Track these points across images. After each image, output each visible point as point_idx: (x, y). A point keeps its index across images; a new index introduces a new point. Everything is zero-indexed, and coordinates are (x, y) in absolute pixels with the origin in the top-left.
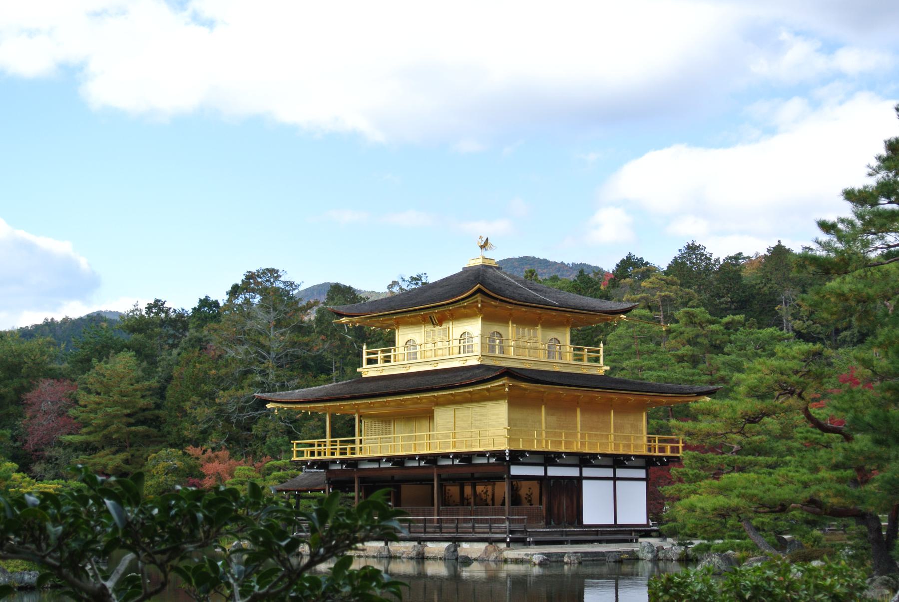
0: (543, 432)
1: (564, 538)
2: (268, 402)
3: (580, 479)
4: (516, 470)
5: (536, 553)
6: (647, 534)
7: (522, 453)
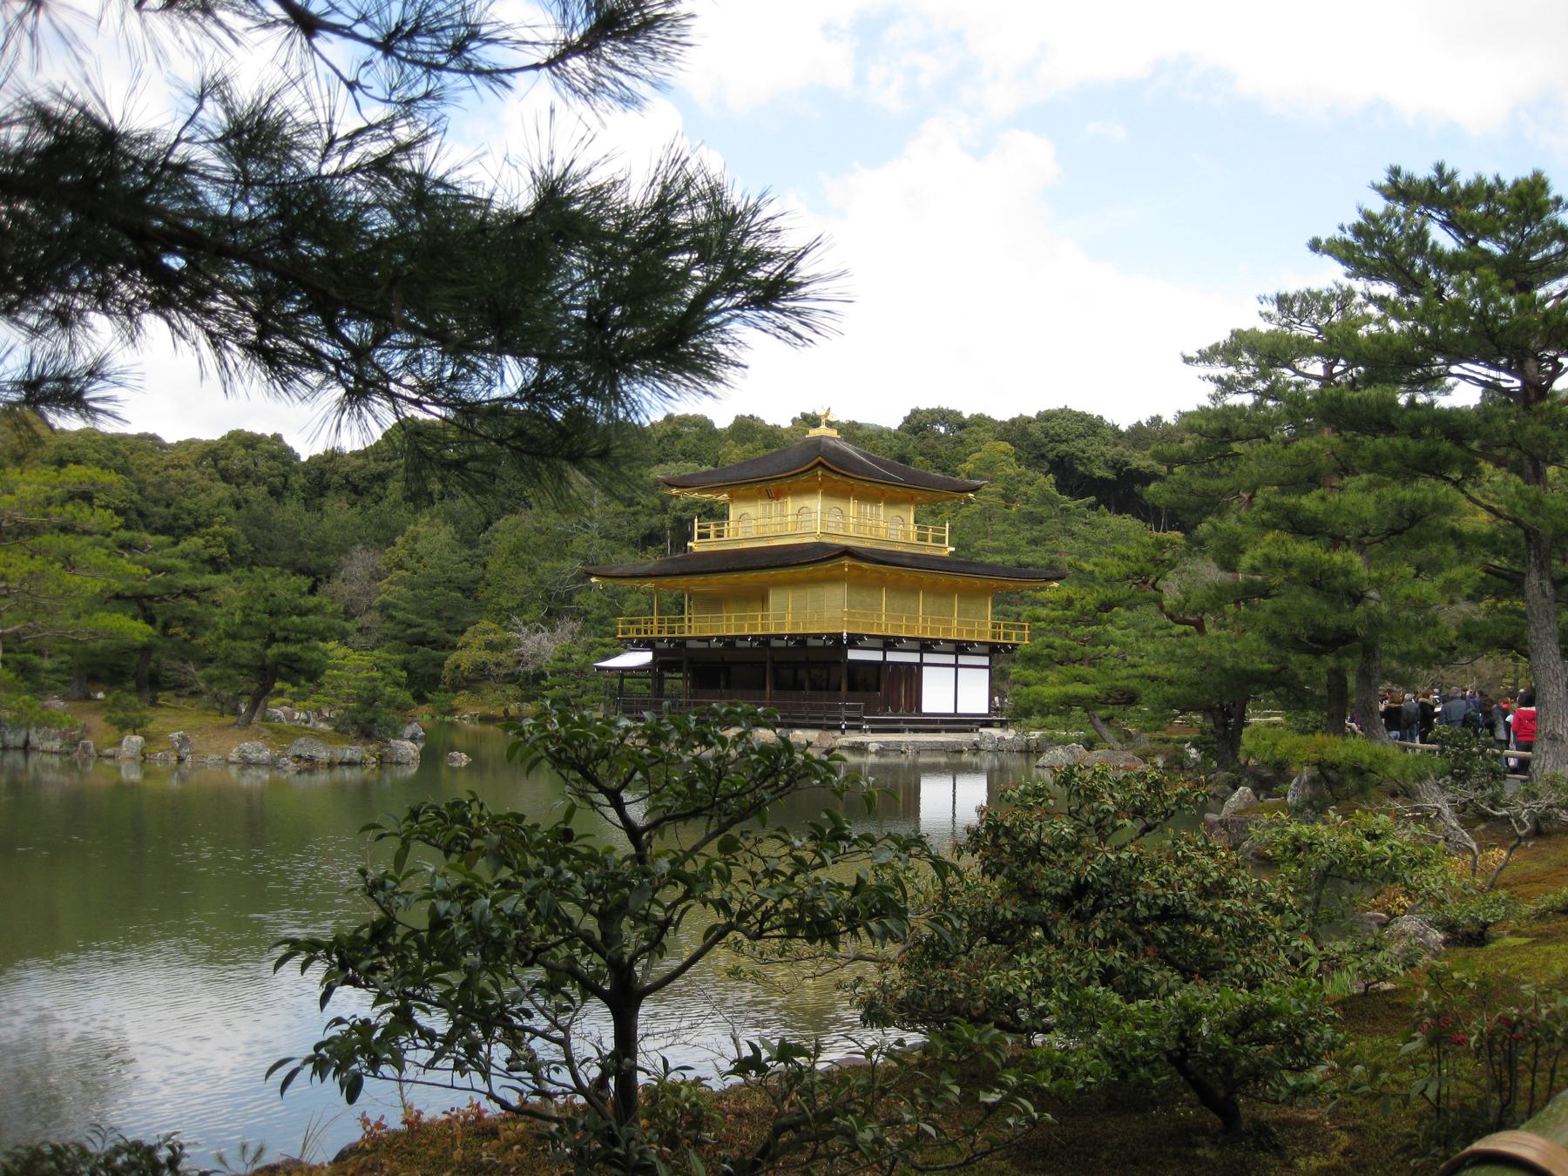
0: (884, 614)
3: (920, 665)
4: (853, 655)
5: (873, 740)
6: (988, 724)
7: (861, 637)
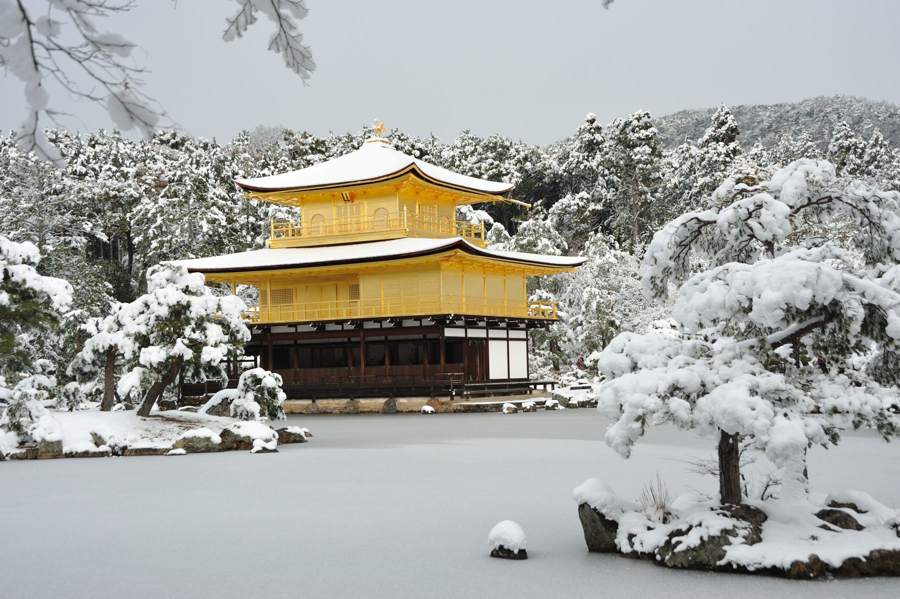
1: (486, 391)
3: (487, 339)
4: (449, 333)
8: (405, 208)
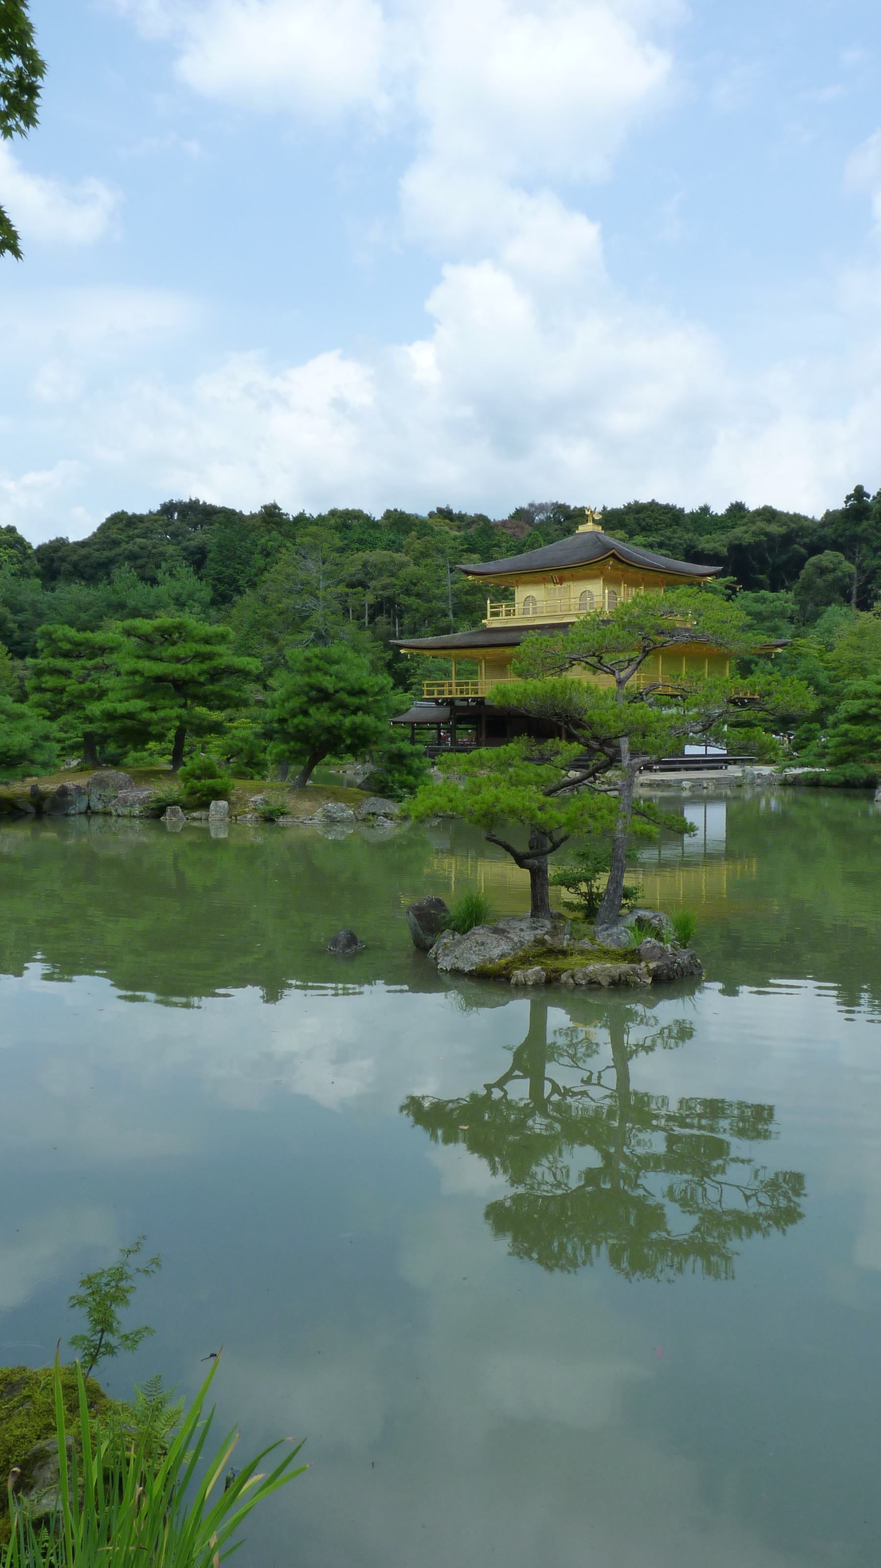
2: (402, 647)
6: (727, 762)
8: (606, 591)
